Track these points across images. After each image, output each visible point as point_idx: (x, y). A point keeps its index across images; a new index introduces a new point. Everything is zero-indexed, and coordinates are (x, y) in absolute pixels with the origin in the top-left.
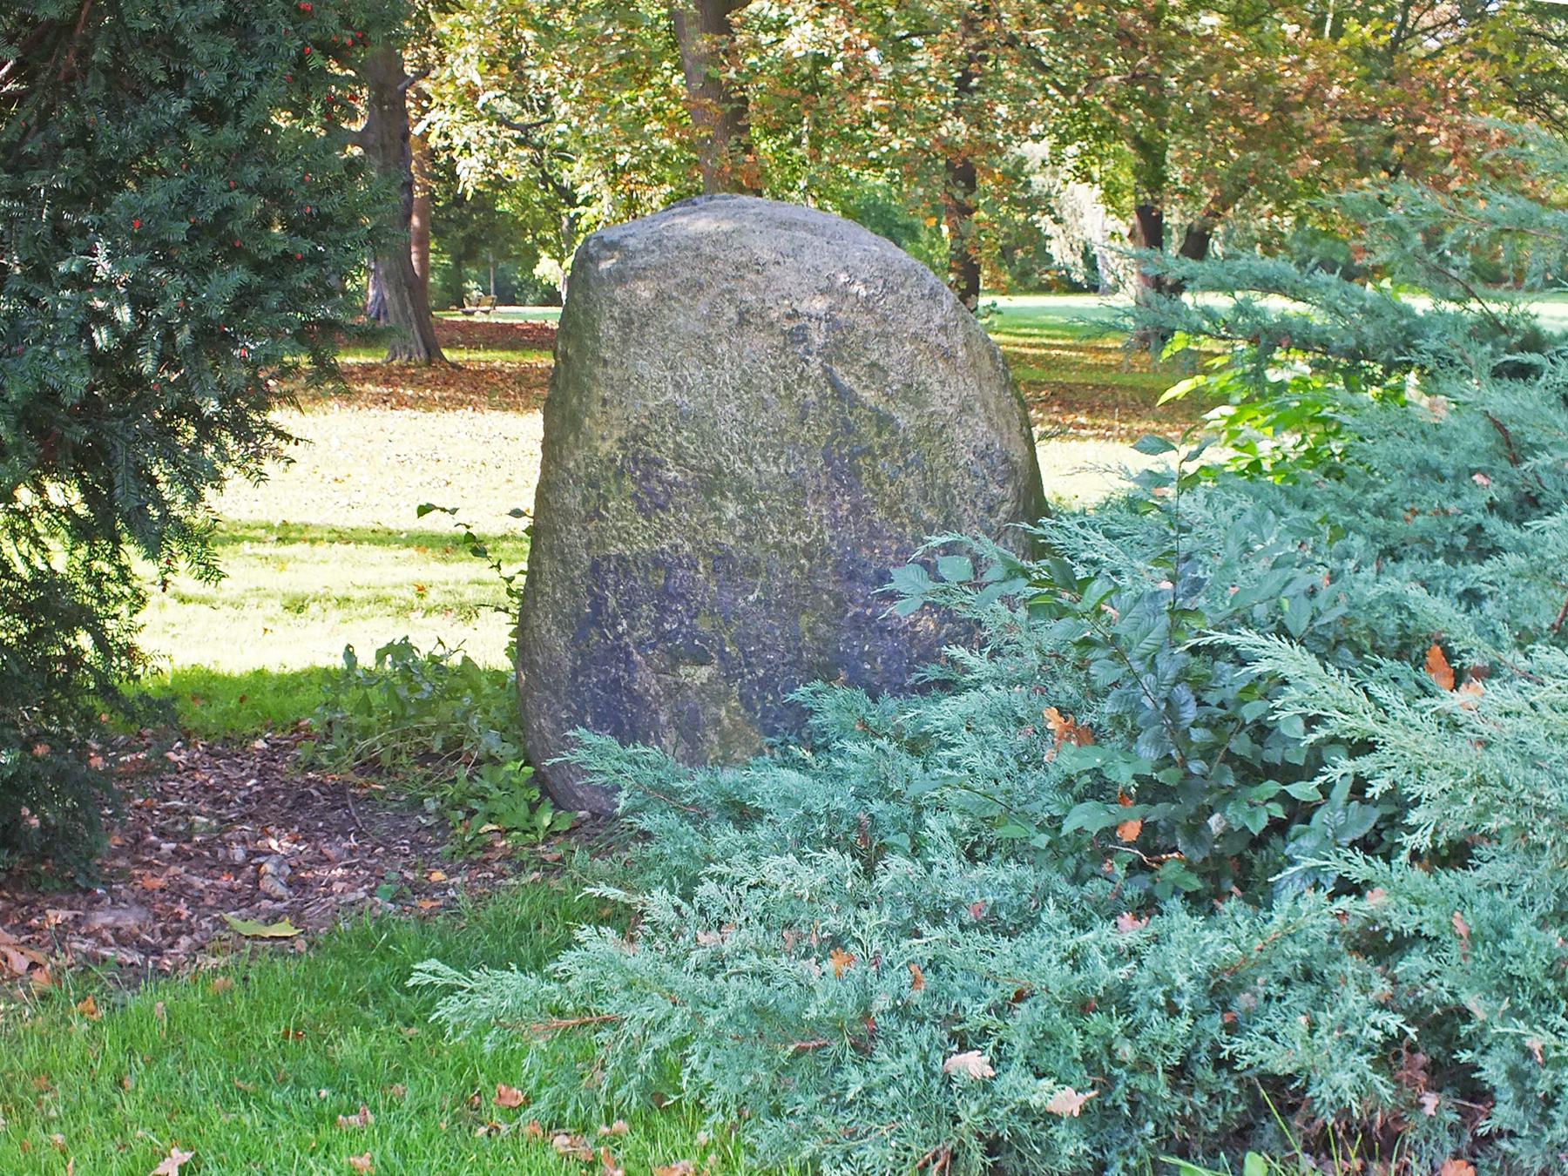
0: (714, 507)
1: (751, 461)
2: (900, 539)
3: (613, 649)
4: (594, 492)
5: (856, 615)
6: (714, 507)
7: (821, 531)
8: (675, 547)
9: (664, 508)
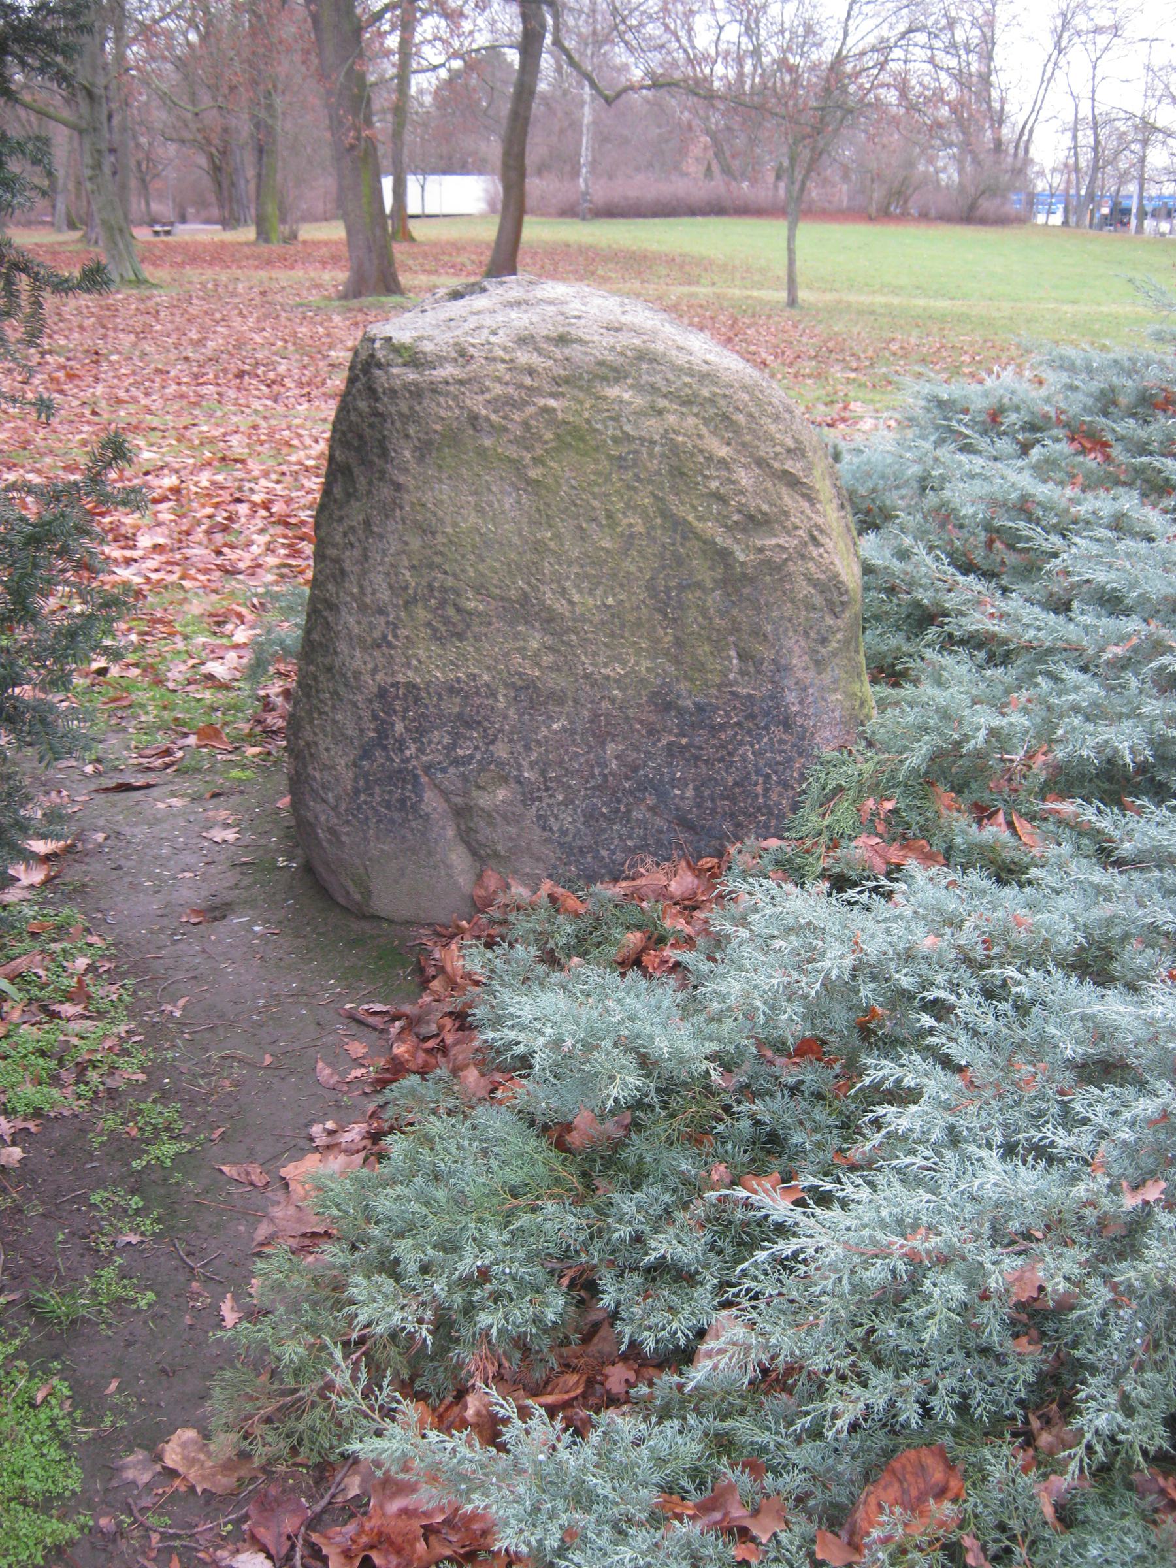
0: (517, 636)
1: (564, 592)
2: (724, 673)
3: (400, 771)
4: (382, 620)
5: (670, 744)
6: (517, 636)
7: (637, 663)
8: (474, 677)
9: (460, 636)
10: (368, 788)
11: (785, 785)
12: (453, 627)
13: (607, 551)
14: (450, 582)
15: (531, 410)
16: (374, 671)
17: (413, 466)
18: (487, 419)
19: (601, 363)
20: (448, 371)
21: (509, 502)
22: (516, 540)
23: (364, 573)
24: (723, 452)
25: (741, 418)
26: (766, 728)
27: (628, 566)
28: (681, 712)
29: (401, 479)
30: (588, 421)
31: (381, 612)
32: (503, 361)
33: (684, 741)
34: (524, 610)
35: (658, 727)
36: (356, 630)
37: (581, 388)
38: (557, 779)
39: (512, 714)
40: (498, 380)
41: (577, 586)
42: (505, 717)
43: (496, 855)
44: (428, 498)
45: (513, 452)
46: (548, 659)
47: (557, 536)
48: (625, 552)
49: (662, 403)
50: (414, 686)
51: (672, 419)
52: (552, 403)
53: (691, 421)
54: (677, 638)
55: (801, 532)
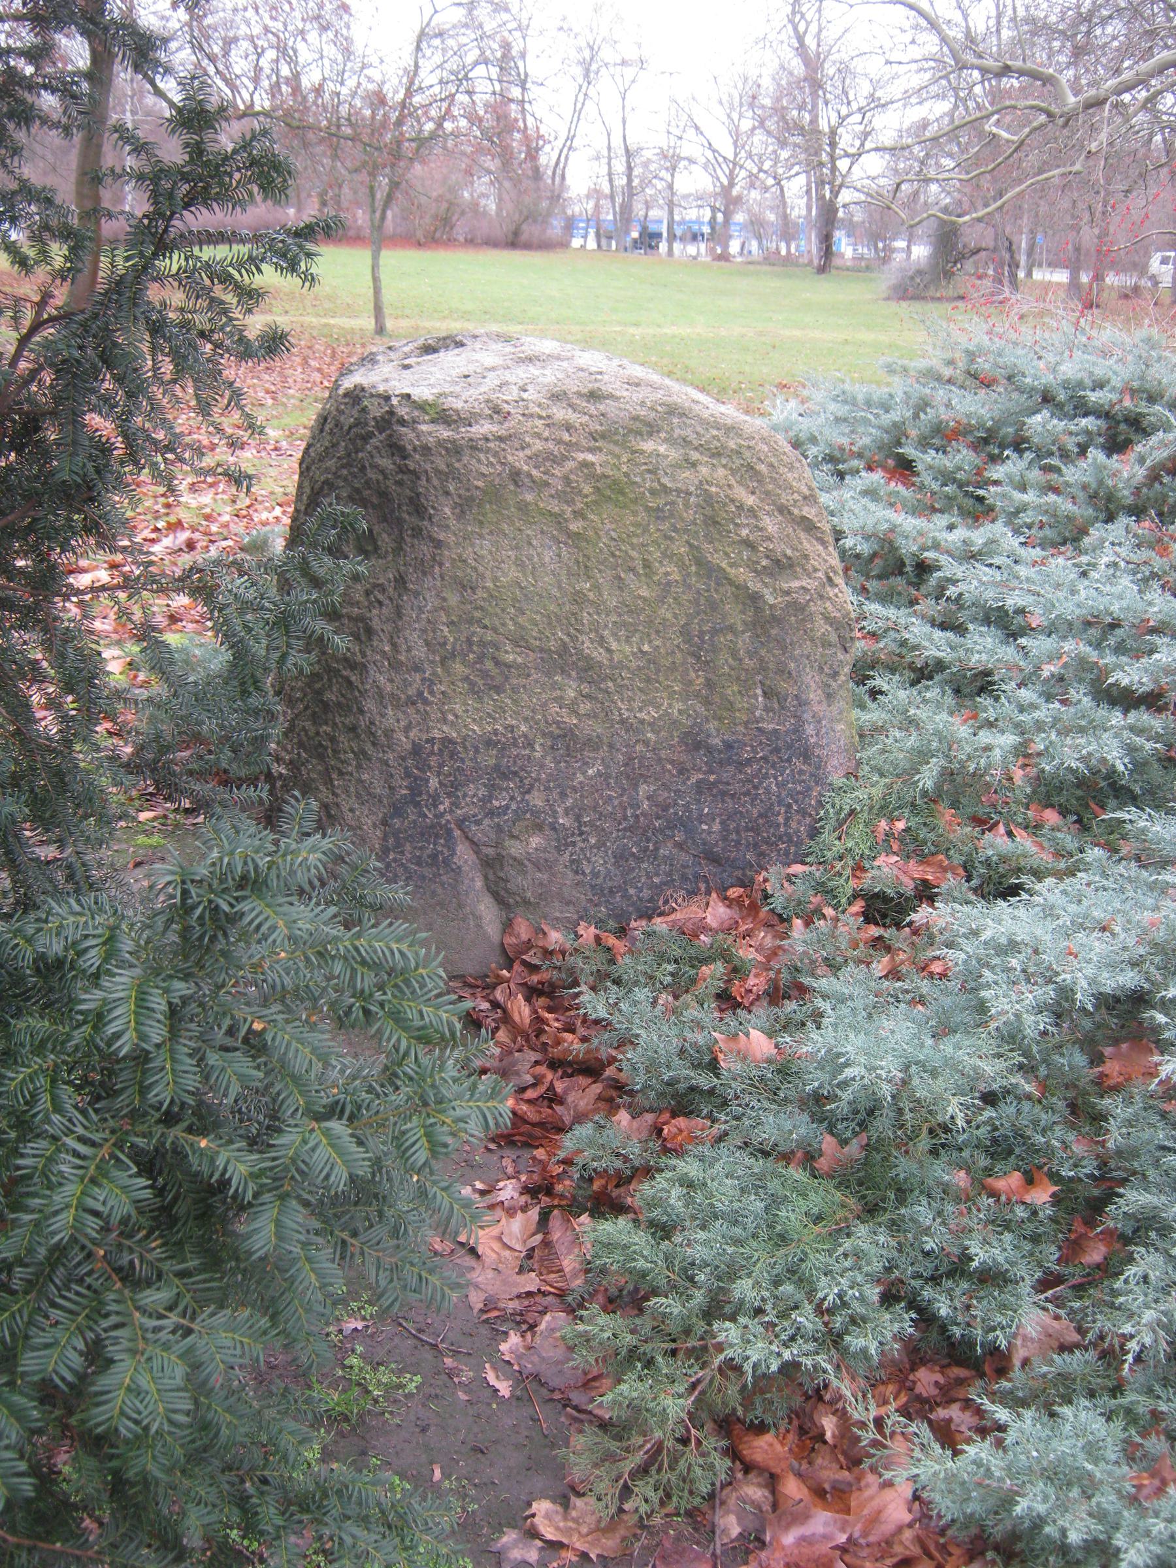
0: (554, 686)
1: (602, 640)
2: (751, 710)
3: (433, 827)
5: (699, 782)
6: (554, 686)
8: (511, 729)
9: (498, 689)
10: (398, 845)
11: (804, 813)
12: (492, 679)
13: (645, 599)
14: (489, 636)
15: (570, 464)
16: (407, 729)
17: (452, 522)
18: (529, 475)
19: (635, 418)
20: (484, 428)
21: (548, 556)
22: (555, 592)
23: (398, 630)
24: (750, 500)
25: (762, 468)
26: (789, 760)
27: (664, 612)
28: (710, 750)
29: (442, 536)
30: (626, 475)
31: (417, 668)
32: (540, 417)
33: (712, 778)
34: (564, 660)
35: (689, 765)
36: (388, 688)
37: (616, 443)
38: (591, 824)
39: (549, 763)
40: (538, 436)
41: (615, 635)
42: (542, 766)
43: (526, 902)
44: (468, 554)
45: (554, 506)
46: (585, 707)
47: (596, 587)
48: (662, 600)
49: (695, 456)
50: (451, 741)
51: (704, 470)
52: (590, 457)
53: (721, 472)
54: (708, 680)
55: (820, 574)
